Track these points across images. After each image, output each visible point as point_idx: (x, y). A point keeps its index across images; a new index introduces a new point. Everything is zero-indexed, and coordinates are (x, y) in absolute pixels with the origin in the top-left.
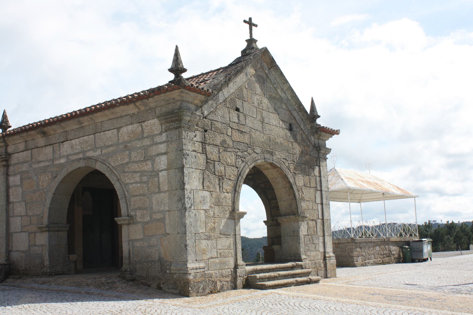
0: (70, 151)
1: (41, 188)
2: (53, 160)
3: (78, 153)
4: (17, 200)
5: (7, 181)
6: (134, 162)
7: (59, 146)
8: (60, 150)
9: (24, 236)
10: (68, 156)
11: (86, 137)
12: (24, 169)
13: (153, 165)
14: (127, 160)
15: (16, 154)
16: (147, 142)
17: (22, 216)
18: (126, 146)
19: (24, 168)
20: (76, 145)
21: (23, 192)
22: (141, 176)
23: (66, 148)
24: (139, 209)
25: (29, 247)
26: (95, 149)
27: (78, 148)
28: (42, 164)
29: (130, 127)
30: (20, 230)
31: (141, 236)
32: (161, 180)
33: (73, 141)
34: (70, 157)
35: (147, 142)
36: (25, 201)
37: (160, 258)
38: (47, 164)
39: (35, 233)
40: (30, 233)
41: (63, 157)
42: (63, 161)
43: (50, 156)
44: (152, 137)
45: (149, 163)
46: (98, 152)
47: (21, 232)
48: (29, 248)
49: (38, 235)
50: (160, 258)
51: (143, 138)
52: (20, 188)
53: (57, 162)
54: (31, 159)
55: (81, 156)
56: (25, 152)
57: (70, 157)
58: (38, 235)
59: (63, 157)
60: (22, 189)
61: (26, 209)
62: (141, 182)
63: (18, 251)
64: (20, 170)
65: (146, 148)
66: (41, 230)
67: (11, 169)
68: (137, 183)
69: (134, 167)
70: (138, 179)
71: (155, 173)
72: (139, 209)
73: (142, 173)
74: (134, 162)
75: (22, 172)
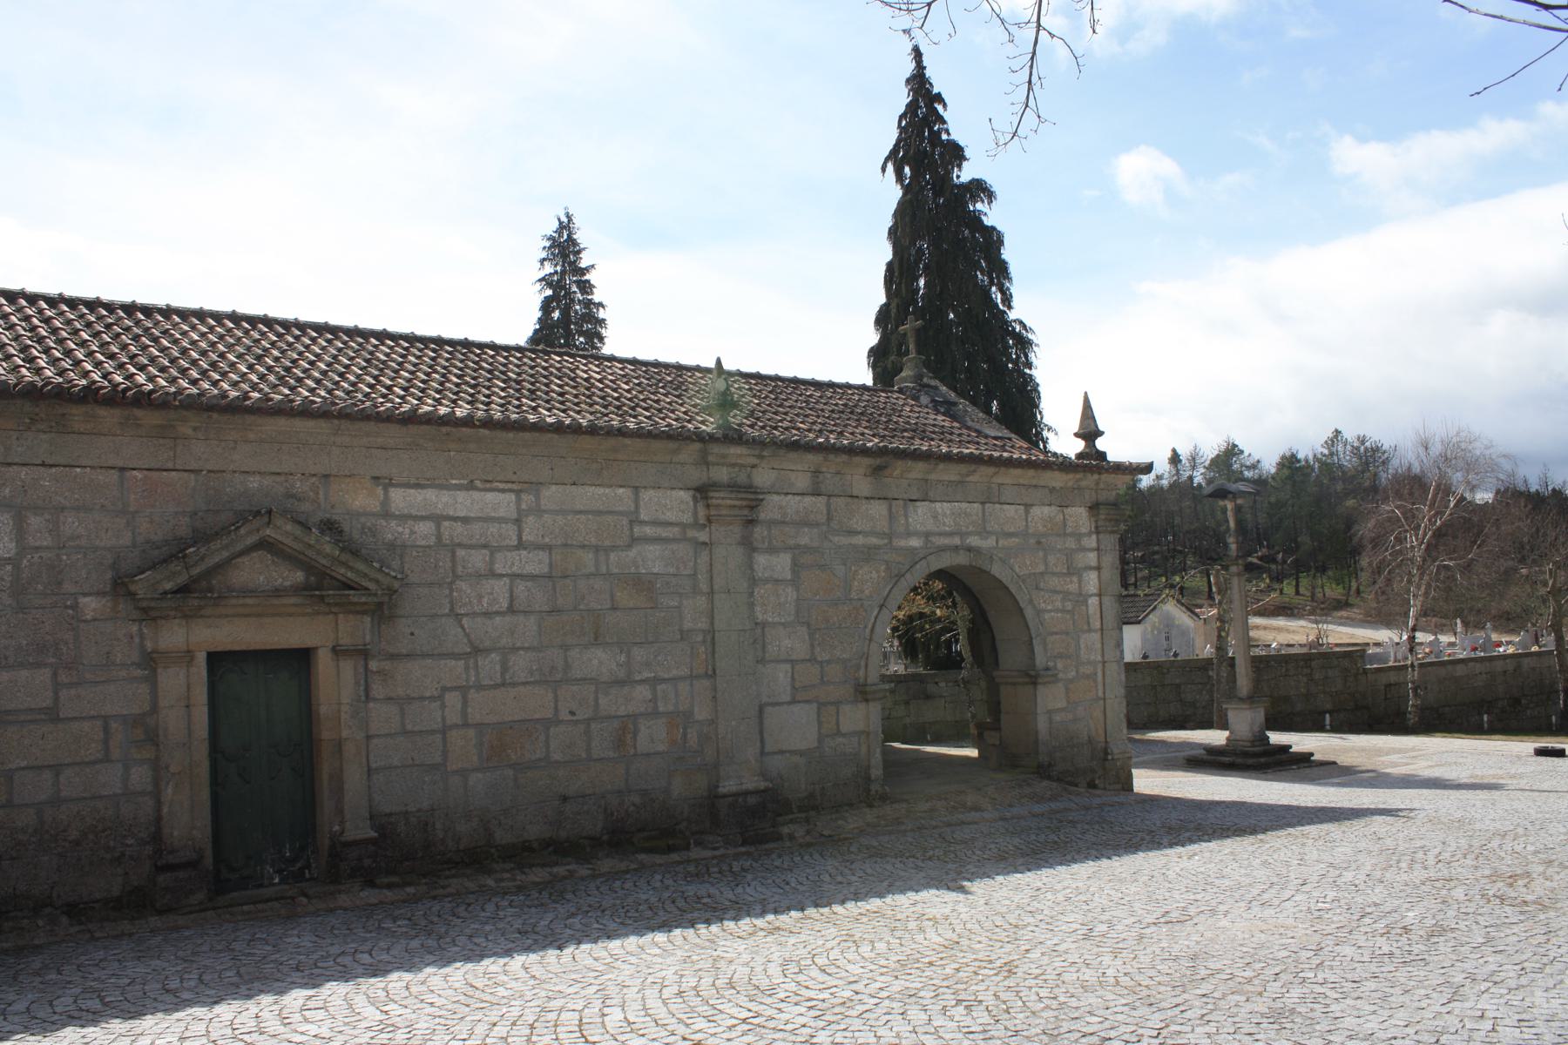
0: (930, 526)
1: (854, 595)
2: (890, 536)
3: (951, 534)
4: (777, 619)
5: (750, 566)
6: (1054, 574)
7: (905, 507)
8: (906, 516)
9: (804, 715)
10: (927, 535)
11: (964, 505)
12: (804, 540)
13: (1080, 582)
14: (1041, 568)
15: (776, 498)
16: (1071, 543)
17: (793, 662)
18: (1039, 543)
19: (806, 538)
20: (944, 515)
21: (798, 599)
22: (1063, 600)
23: (921, 516)
24: (1060, 656)
25: (820, 740)
26: (983, 533)
27: (948, 524)
28: (859, 540)
29: (1046, 509)
30: (789, 699)
31: (1061, 704)
32: (1091, 610)
33: (938, 505)
34: (933, 539)
35: (1071, 543)
36: (809, 625)
37: (1090, 741)
38: (874, 541)
39: (837, 703)
40: (822, 705)
41: (916, 534)
42: (915, 542)
43: (883, 525)
44: (1079, 537)
45: (1075, 579)
46: (990, 542)
47: (793, 702)
48: (819, 741)
49: (846, 709)
50: (1090, 741)
51: (1065, 534)
52: (789, 590)
53: (902, 543)
54: (829, 519)
55: (957, 541)
56: (808, 499)
57: (933, 539)
58: (846, 709)
59: (916, 534)
60: (798, 590)
61: (812, 646)
62: (1063, 611)
63: (782, 752)
64: (792, 542)
65: (1069, 555)
66: (862, 693)
67: (759, 532)
68: (1057, 610)
69: (1054, 582)
70: (1059, 604)
71: (1082, 598)
72: (1060, 656)
73: (1066, 595)
74: (1054, 574)
75: (797, 547)
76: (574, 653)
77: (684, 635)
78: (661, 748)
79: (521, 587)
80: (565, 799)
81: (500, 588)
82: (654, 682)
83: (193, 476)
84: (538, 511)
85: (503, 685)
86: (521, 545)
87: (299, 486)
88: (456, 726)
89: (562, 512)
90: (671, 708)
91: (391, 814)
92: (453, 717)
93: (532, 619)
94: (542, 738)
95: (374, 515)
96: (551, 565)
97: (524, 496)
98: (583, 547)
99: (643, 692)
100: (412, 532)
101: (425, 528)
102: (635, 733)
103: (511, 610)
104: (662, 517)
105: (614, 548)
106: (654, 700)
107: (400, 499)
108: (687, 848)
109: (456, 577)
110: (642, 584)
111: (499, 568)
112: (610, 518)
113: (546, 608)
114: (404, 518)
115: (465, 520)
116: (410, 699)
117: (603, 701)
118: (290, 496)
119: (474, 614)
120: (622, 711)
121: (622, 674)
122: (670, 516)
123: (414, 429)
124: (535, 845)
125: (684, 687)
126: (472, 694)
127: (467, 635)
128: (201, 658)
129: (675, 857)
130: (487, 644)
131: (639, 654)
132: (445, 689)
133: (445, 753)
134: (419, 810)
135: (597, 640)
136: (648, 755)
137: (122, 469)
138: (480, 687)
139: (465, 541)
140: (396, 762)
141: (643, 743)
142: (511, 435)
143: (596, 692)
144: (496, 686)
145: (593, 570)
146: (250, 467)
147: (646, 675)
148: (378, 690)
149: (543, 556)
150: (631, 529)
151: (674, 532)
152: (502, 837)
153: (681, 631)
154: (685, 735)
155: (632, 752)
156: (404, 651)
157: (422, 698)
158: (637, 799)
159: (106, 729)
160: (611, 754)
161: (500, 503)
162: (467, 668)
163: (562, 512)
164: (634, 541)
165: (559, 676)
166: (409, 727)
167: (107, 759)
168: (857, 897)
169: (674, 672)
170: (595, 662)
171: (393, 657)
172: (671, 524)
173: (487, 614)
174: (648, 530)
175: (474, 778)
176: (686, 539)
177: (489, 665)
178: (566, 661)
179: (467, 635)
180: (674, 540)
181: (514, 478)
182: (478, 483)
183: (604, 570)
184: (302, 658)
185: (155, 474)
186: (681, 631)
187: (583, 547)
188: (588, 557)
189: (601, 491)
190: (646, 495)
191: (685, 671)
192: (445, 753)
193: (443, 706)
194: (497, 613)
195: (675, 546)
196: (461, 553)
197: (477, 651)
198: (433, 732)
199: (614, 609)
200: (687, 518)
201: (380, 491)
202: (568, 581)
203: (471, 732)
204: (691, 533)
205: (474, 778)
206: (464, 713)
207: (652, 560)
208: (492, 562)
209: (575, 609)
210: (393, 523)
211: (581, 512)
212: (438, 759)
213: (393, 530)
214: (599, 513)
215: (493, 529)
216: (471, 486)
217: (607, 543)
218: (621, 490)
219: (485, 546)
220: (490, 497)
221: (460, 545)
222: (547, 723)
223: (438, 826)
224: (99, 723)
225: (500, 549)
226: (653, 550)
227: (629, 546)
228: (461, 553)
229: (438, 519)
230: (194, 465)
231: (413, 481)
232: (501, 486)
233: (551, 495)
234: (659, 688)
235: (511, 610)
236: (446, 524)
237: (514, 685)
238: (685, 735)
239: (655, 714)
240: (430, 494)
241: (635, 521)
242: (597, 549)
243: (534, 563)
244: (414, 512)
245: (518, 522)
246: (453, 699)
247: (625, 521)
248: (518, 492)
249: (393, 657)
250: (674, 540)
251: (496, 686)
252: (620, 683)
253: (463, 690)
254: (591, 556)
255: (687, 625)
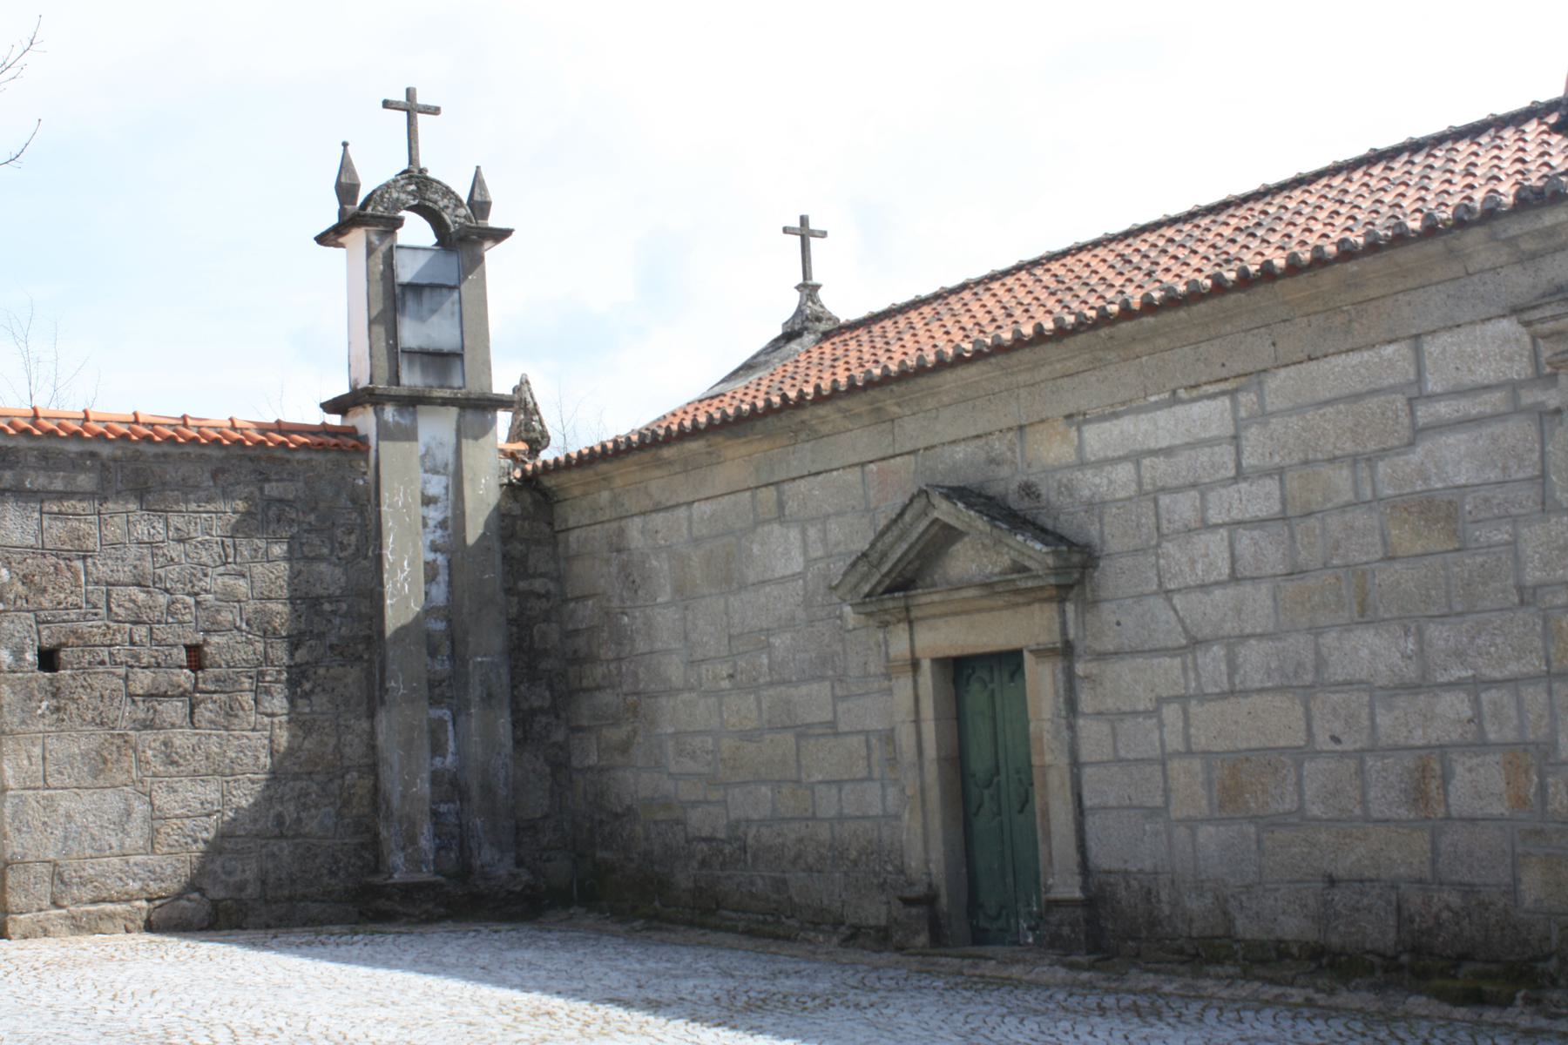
76: (1330, 639)
77: (1527, 596)
78: (1498, 809)
79: (1245, 539)
80: (1332, 881)
81: (1216, 544)
82: (1475, 686)
83: (912, 458)
84: (1263, 416)
85: (1232, 692)
86: (1240, 475)
87: (999, 446)
88: (1178, 754)
89: (1298, 410)
90: (1510, 735)
91: (1110, 872)
92: (1175, 742)
93: (1265, 588)
94: (1292, 778)
95: (1069, 467)
96: (1284, 501)
97: (1243, 398)
98: (1333, 460)
99: (1454, 705)
100: (1110, 482)
101: (1124, 472)
102: (1446, 778)
103: (1235, 578)
104: (1468, 380)
105: (1384, 452)
106: (1477, 718)
107: (1099, 438)
108: (1506, 1002)
109: (1161, 536)
110: (1439, 510)
111: (1214, 516)
112: (1374, 403)
113: (1281, 569)
114: (1101, 463)
115: (1168, 452)
116: (1122, 714)
117: (1383, 720)
118: (992, 461)
119: (1188, 589)
120: (1418, 738)
121: (1411, 672)
122: (1485, 373)
123: (1071, 342)
124: (1295, 950)
125: (1535, 696)
126: (1194, 707)
127: (1181, 621)
128: (926, 665)
129: (1490, 1015)
130: (1207, 631)
131: (1439, 635)
132: (1161, 701)
133: (1167, 792)
134: (1141, 871)
135: (1365, 615)
136: (1473, 820)
137: (863, 464)
138: (1203, 698)
139: (1171, 482)
140: (1112, 802)
141: (1461, 796)
142: (1182, 314)
143: (1372, 707)
144: (1223, 696)
145: (1348, 496)
146: (953, 436)
147: (1458, 673)
148: (1086, 702)
149: (1272, 485)
150: (1412, 413)
151: (1494, 401)
152: (1245, 928)
153: (1521, 589)
154: (1543, 788)
155: (1441, 812)
156: (1111, 648)
157: (1135, 713)
158: (1455, 900)
159: (867, 742)
160: (1403, 813)
161: (1208, 415)
162: (1185, 669)
163: (1298, 410)
164: (1418, 433)
165: (1308, 678)
166: (1122, 753)
167: (869, 778)
168: (544, 990)
169: (1513, 668)
170: (1364, 653)
171: (1101, 656)
172: (1488, 388)
173: (1203, 587)
174: (1443, 409)
175: (1206, 833)
176: (1518, 410)
177: (1212, 660)
178: (1317, 652)
179: (1181, 621)
180: (1497, 417)
181: (1224, 373)
182: (1182, 393)
183: (1368, 495)
184: (1009, 662)
185: (884, 464)
186: (1521, 589)
187: (1333, 460)
188: (1341, 478)
189: (1354, 358)
190: (1432, 347)
191: (1534, 664)
192: (1167, 792)
193: (1161, 725)
194: (1217, 584)
195: (1497, 428)
196: (1165, 500)
197: (1195, 643)
198: (1148, 761)
199: (1389, 558)
200: (1520, 369)
201: (1073, 433)
202: (1312, 521)
203: (1197, 764)
204: (1528, 397)
205: (1206, 833)
206: (1187, 738)
207: (1455, 461)
208: (1204, 508)
209: (1325, 566)
210: (1089, 473)
211: (1327, 403)
212: (1159, 801)
213: (1091, 483)
214: (1357, 397)
215: (1204, 456)
216: (1174, 400)
217: (1372, 446)
218: (1389, 350)
219: (1194, 486)
220: (1198, 409)
221: (1163, 490)
222: (1303, 754)
223: (1164, 896)
224: (863, 738)
225: (1211, 486)
226: (1455, 443)
227: (1411, 444)
228: (1165, 500)
229: (1136, 457)
230: (908, 447)
231: (1108, 410)
232: (1211, 389)
233: (1279, 381)
234: (1485, 697)
235: (1235, 578)
236: (1146, 462)
237: (1246, 693)
238: (1543, 788)
239: (1480, 745)
240: (1126, 424)
241: (1417, 395)
242: (1354, 459)
243: (1260, 499)
244: (1110, 454)
245: (1236, 438)
246: (1171, 713)
247: (1400, 402)
248: (1231, 393)
249: (1101, 656)
250: (1497, 417)
251: (1223, 696)
252: (1413, 688)
253: (1183, 699)
254: (1346, 472)
255: (1532, 575)
